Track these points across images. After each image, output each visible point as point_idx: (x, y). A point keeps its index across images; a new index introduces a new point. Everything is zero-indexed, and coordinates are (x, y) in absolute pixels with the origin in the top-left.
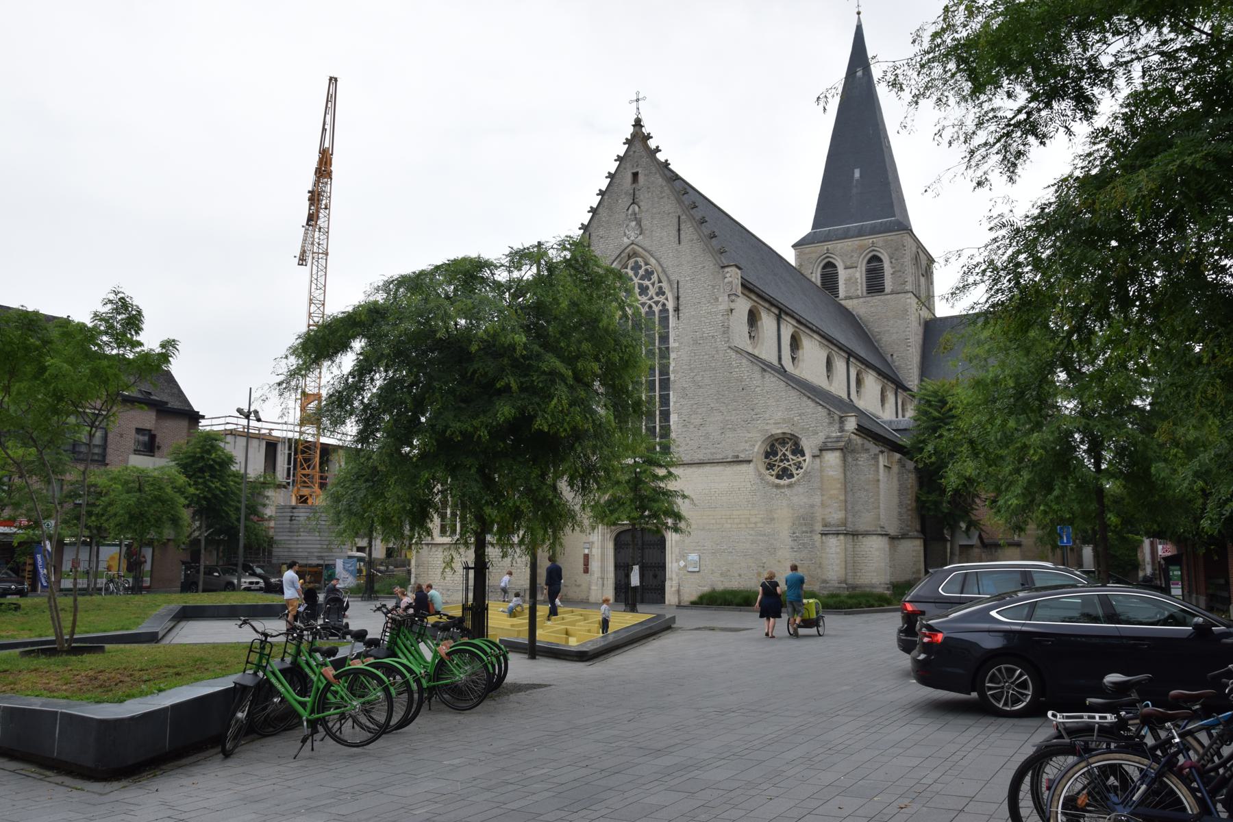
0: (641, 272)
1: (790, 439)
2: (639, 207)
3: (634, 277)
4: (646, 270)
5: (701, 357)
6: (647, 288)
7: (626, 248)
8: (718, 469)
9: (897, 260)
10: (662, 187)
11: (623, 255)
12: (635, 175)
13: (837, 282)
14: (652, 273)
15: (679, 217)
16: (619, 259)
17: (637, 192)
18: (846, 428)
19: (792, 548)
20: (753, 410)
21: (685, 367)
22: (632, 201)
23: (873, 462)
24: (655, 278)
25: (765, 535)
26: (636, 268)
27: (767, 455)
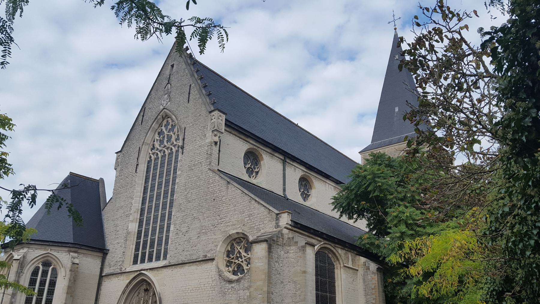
0: (170, 127)
1: (244, 238)
2: (171, 85)
4: (172, 125)
5: (192, 179)
7: (160, 112)
10: (184, 69)
11: (159, 117)
12: (172, 66)
15: (190, 85)
16: (156, 120)
17: (171, 76)
18: (280, 224)
20: (219, 216)
21: (182, 188)
22: (167, 82)
23: (300, 254)
27: (228, 253)
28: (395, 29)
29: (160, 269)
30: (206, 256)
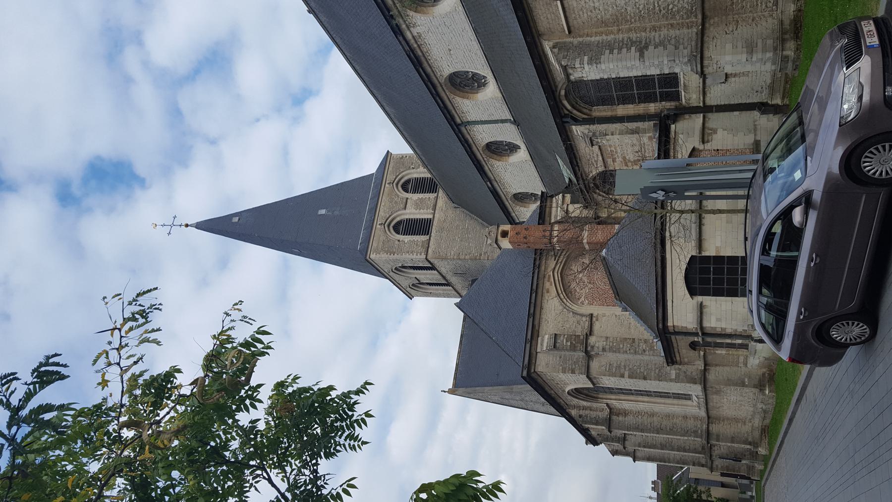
9: (412, 164)
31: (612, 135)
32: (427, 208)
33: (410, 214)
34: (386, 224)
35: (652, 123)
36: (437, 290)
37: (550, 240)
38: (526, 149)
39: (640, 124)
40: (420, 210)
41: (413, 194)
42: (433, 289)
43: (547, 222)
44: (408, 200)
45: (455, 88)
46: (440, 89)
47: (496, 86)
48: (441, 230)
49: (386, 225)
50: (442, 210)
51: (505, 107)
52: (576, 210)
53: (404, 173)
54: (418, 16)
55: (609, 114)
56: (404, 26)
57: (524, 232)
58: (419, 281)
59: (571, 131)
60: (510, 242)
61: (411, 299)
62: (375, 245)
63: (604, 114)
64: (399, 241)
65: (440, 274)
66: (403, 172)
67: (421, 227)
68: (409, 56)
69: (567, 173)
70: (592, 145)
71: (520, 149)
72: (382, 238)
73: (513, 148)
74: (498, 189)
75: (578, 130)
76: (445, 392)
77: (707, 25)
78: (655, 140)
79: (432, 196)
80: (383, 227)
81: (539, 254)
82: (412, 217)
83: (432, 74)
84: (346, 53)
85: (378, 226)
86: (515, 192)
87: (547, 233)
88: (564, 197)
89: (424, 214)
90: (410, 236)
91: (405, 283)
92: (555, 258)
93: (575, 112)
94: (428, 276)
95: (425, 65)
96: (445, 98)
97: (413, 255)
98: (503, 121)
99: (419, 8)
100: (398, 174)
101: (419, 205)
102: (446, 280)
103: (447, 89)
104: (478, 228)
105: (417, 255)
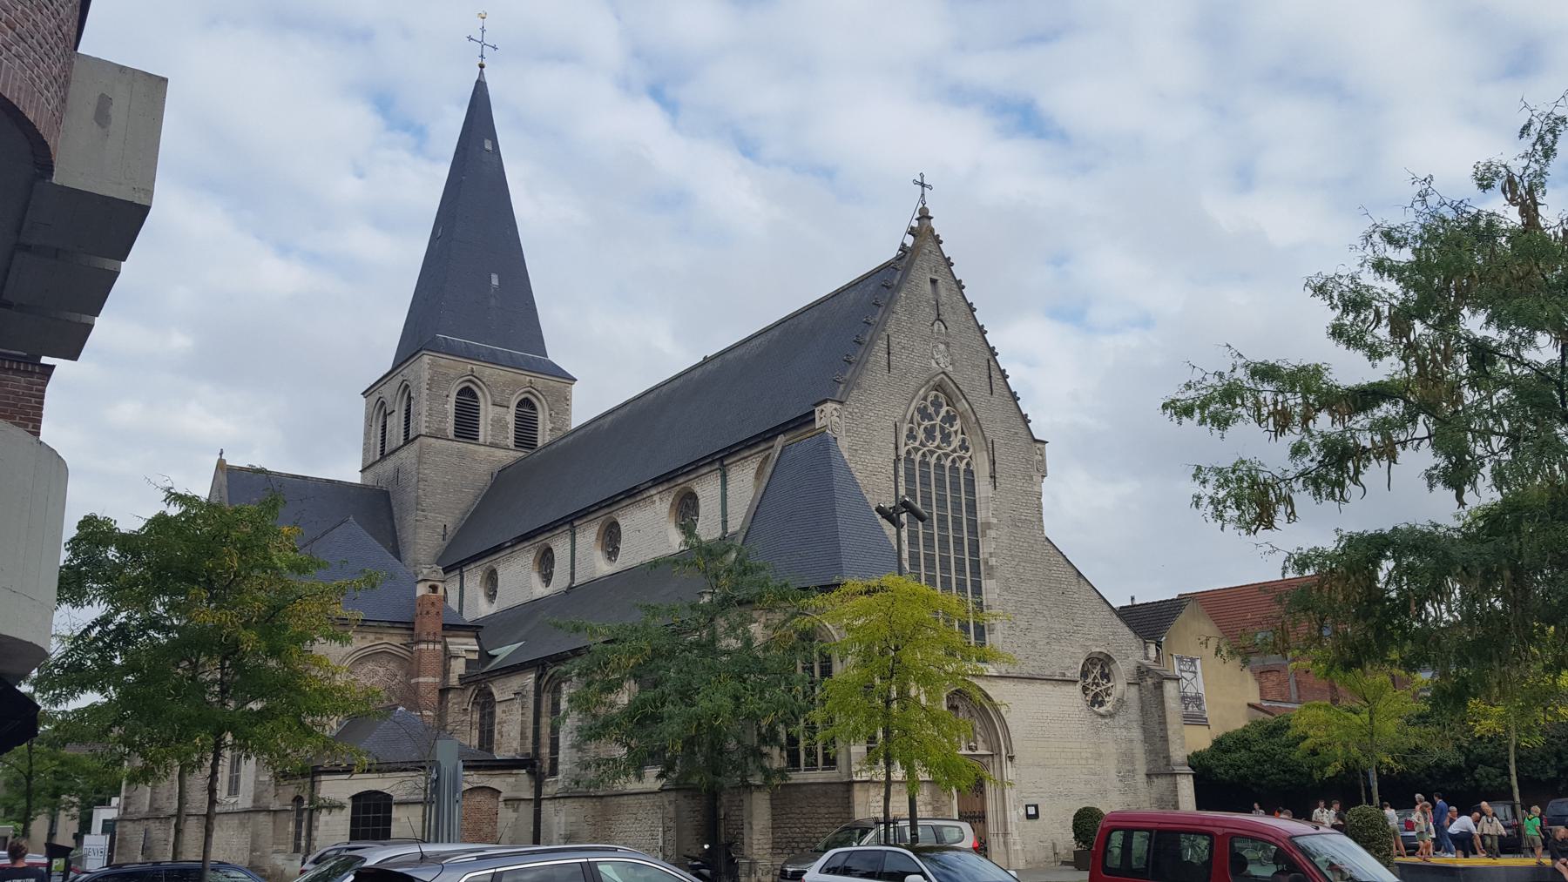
2: (946, 328)
3: (940, 418)
4: (948, 412)
6: (949, 435)
8: (1048, 687)
9: (557, 414)
12: (933, 282)
13: (476, 419)
14: (954, 418)
16: (927, 386)
19: (1120, 791)
24: (957, 425)
25: (1095, 774)
26: (937, 404)
28: (482, 66)
29: (992, 679)
30: (1064, 675)
31: (522, 714)
32: (493, 436)
33: (486, 411)
34: (473, 377)
35: (531, 751)
36: (375, 437)
37: (424, 641)
38: (545, 595)
39: (530, 739)
40: (491, 425)
41: (514, 415)
42: (376, 429)
43: (445, 633)
44: (506, 409)
45: (608, 526)
46: (606, 510)
47: (607, 573)
48: (462, 456)
49: (471, 377)
50: (490, 456)
51: (585, 579)
52: (458, 667)
53: (544, 402)
54: (668, 506)
55: (544, 710)
56: (661, 489)
57: (433, 611)
58: (389, 414)
59: (531, 672)
60: (423, 595)
61: (363, 394)
62: (443, 362)
63: (544, 704)
64: (447, 396)
65: (399, 448)
66: (546, 400)
67: (466, 426)
68: (634, 488)
69: (503, 652)
70: (515, 694)
71: (547, 586)
72: (452, 373)
73: (547, 579)
74: (503, 553)
75: (529, 679)
76: (221, 454)
77: (594, 800)
78: (514, 754)
79: (511, 442)
80: (469, 373)
81: (409, 626)
82: (482, 413)
83: (620, 506)
84: (666, 387)
85: (469, 367)
86: (499, 572)
87: (431, 638)
88: (476, 651)
89: (485, 430)
90: (454, 411)
91: (388, 392)
92: (405, 645)
93: (547, 678)
94: (396, 429)
95: (628, 501)
96: (599, 514)
97: (426, 416)
98: (572, 575)
99: (674, 508)
100: (544, 394)
101: (499, 423)
102: (389, 455)
103: (607, 518)
104: (462, 506)
105: (426, 421)
